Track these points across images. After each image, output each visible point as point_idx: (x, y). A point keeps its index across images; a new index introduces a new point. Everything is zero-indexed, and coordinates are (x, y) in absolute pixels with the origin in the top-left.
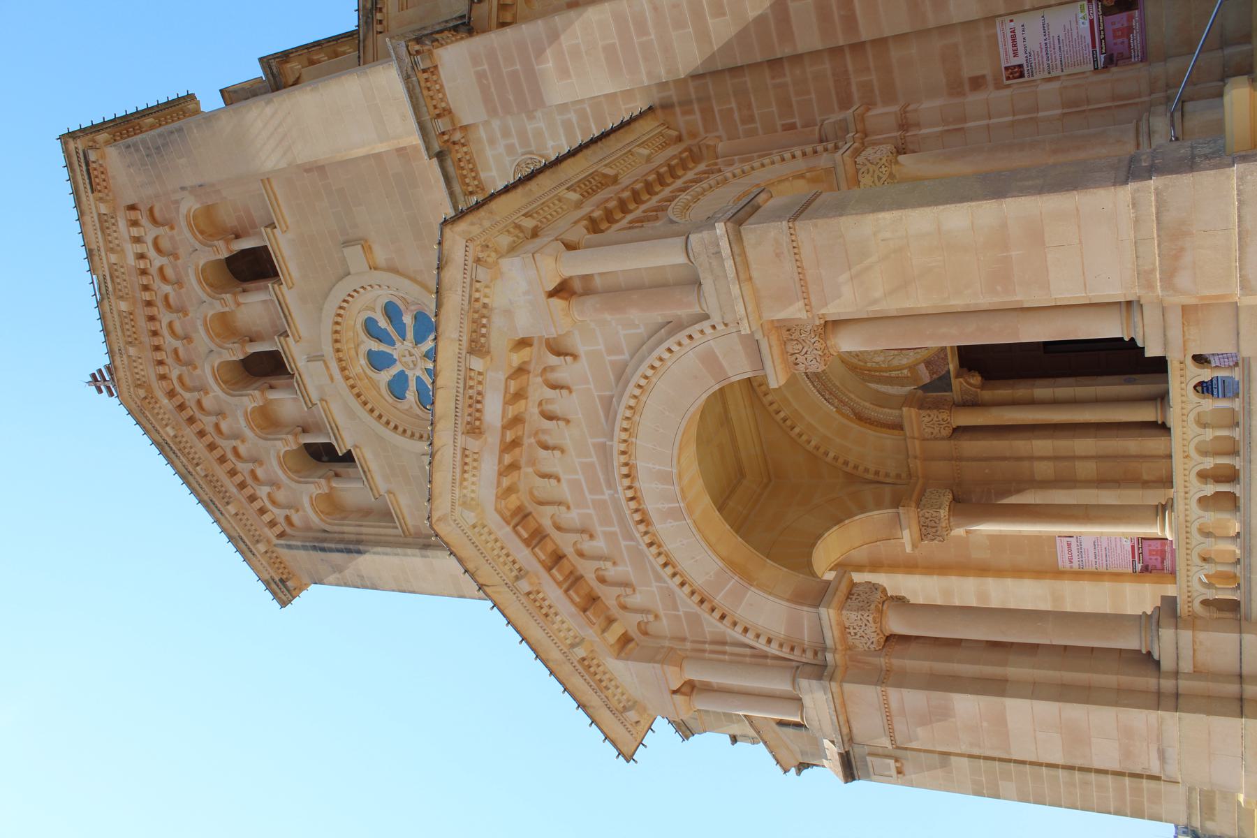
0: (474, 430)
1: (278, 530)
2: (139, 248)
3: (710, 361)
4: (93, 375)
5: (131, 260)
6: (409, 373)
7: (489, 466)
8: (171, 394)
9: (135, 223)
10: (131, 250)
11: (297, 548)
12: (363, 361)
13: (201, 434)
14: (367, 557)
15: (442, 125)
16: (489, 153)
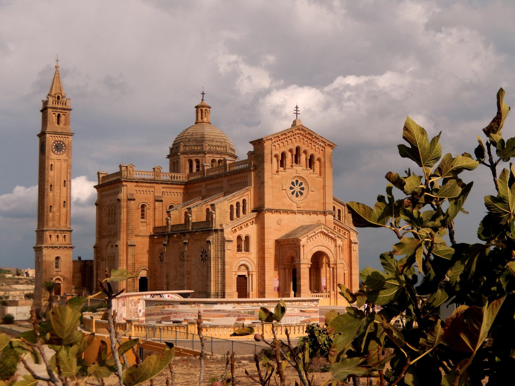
0: (331, 232)
1: (274, 142)
2: (319, 145)
3: (331, 257)
4: (298, 108)
5: (318, 142)
6: (295, 187)
7: (326, 232)
8: (298, 133)
9: (322, 146)
10: (320, 143)
11: (271, 147)
12: (297, 179)
13: (291, 136)
14: (271, 164)
15: (327, 214)
16: (322, 217)
